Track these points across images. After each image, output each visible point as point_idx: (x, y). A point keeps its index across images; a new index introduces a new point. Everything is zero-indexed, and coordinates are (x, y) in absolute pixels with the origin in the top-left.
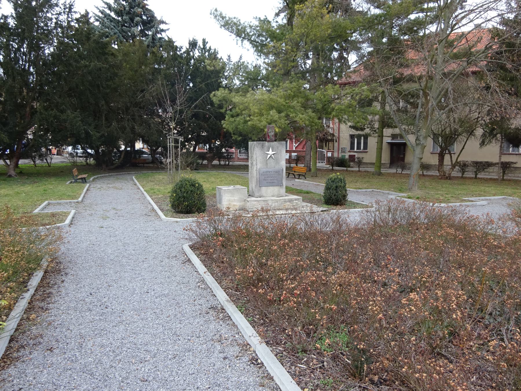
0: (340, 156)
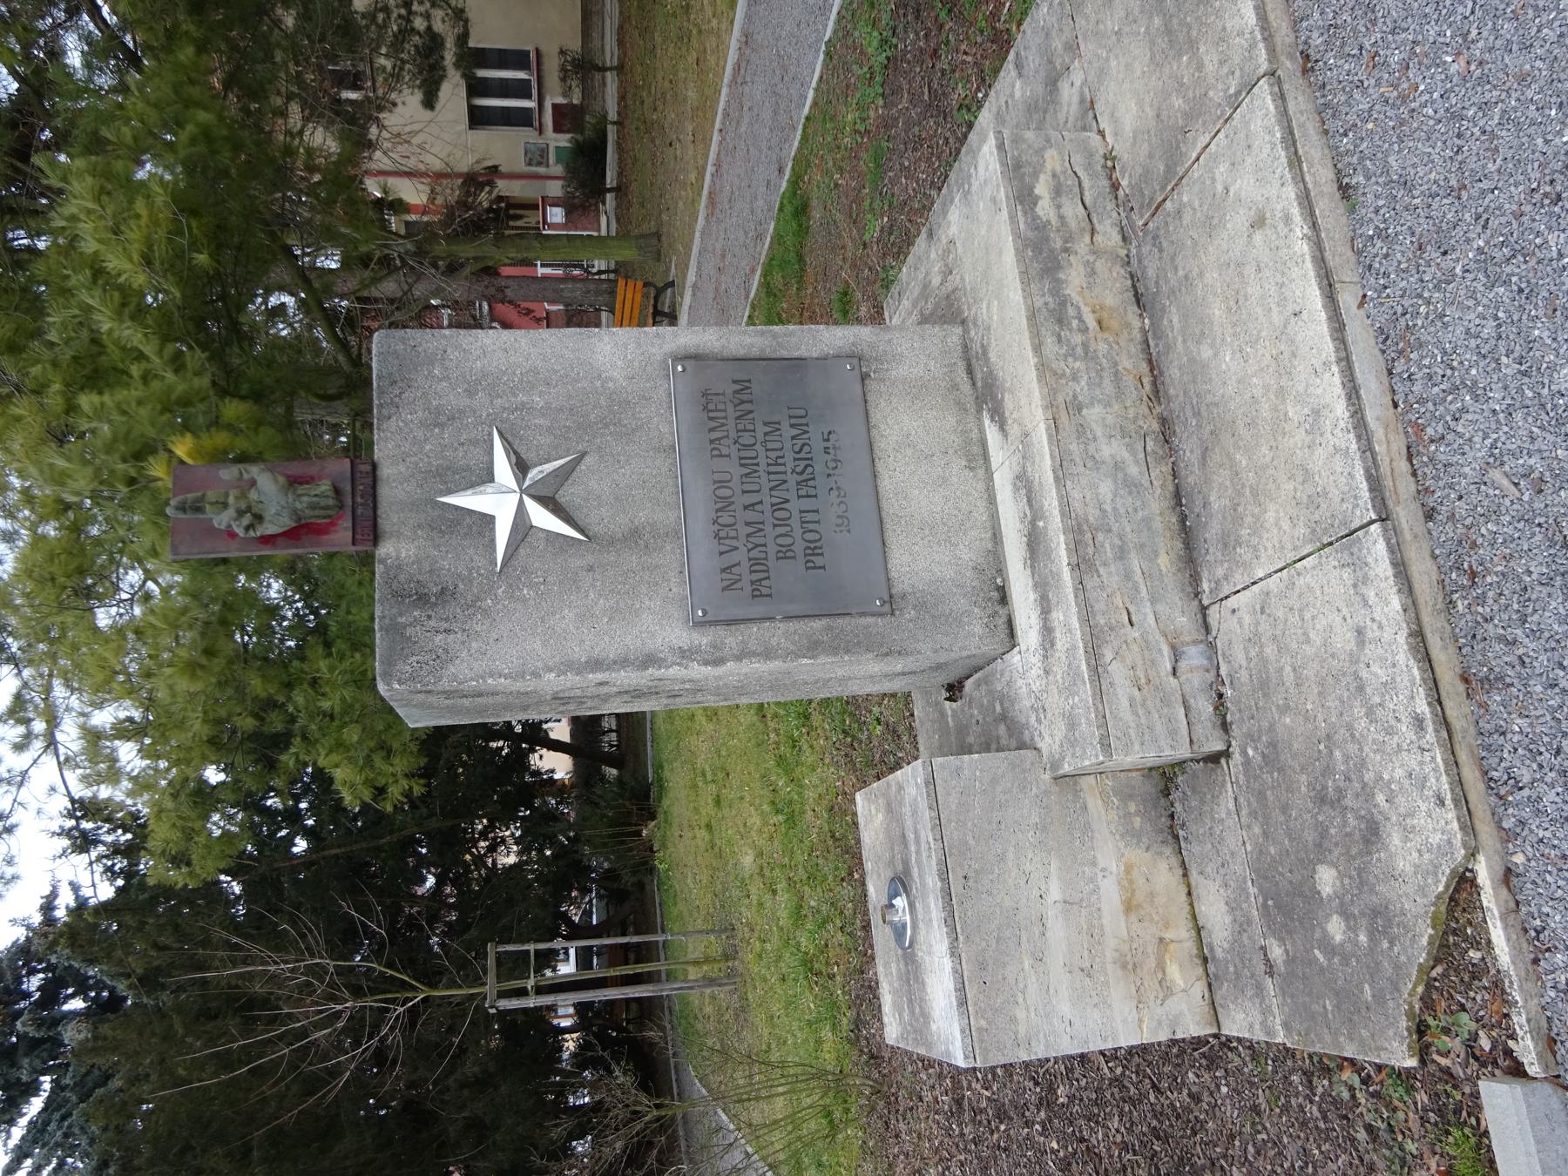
0: (558, 170)
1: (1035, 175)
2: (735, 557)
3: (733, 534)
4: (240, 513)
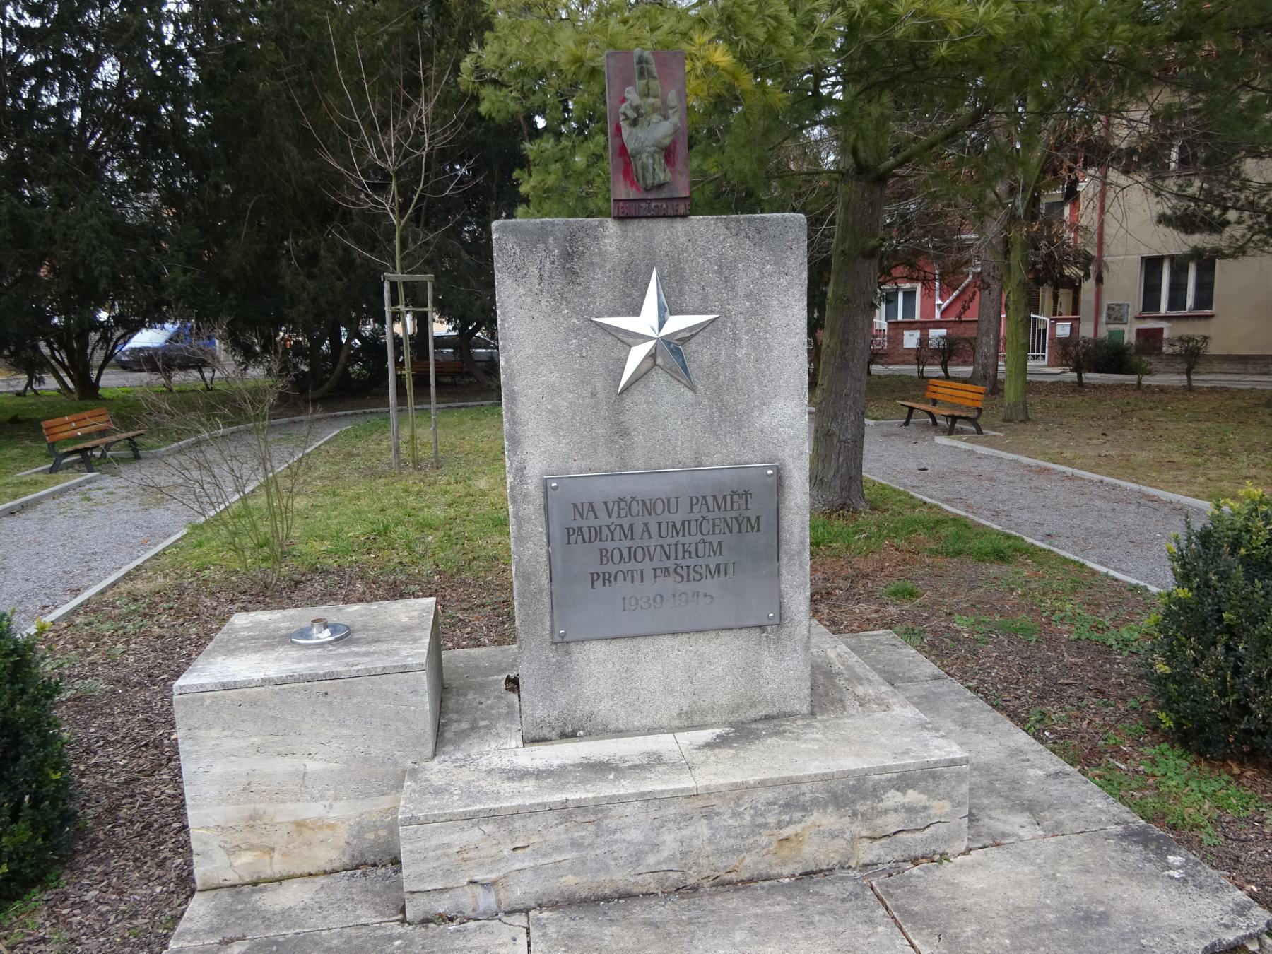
0: (1103, 333)
2: (603, 515)
3: (623, 514)
4: (636, 109)
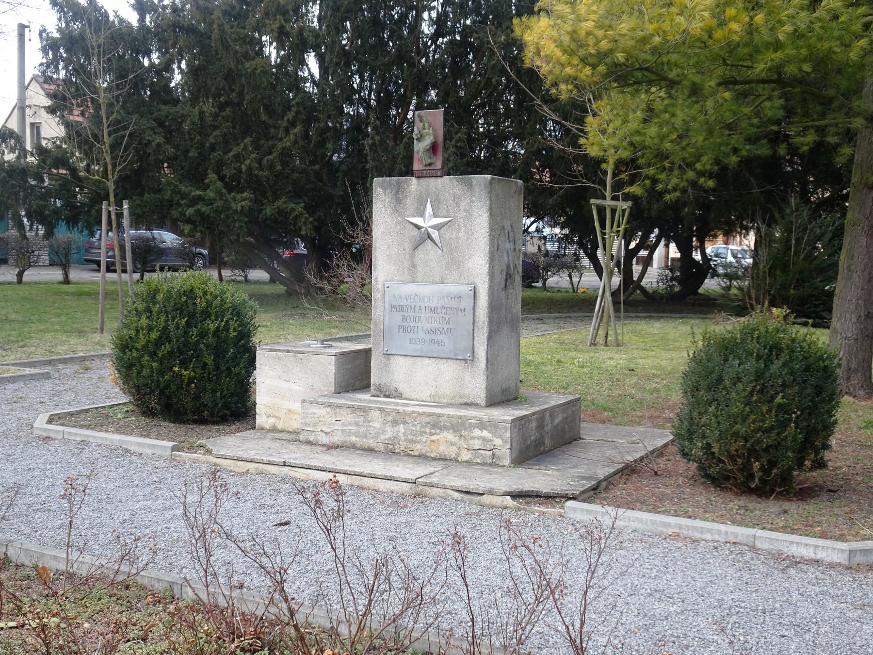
1: (490, 432)
2: (405, 301)
